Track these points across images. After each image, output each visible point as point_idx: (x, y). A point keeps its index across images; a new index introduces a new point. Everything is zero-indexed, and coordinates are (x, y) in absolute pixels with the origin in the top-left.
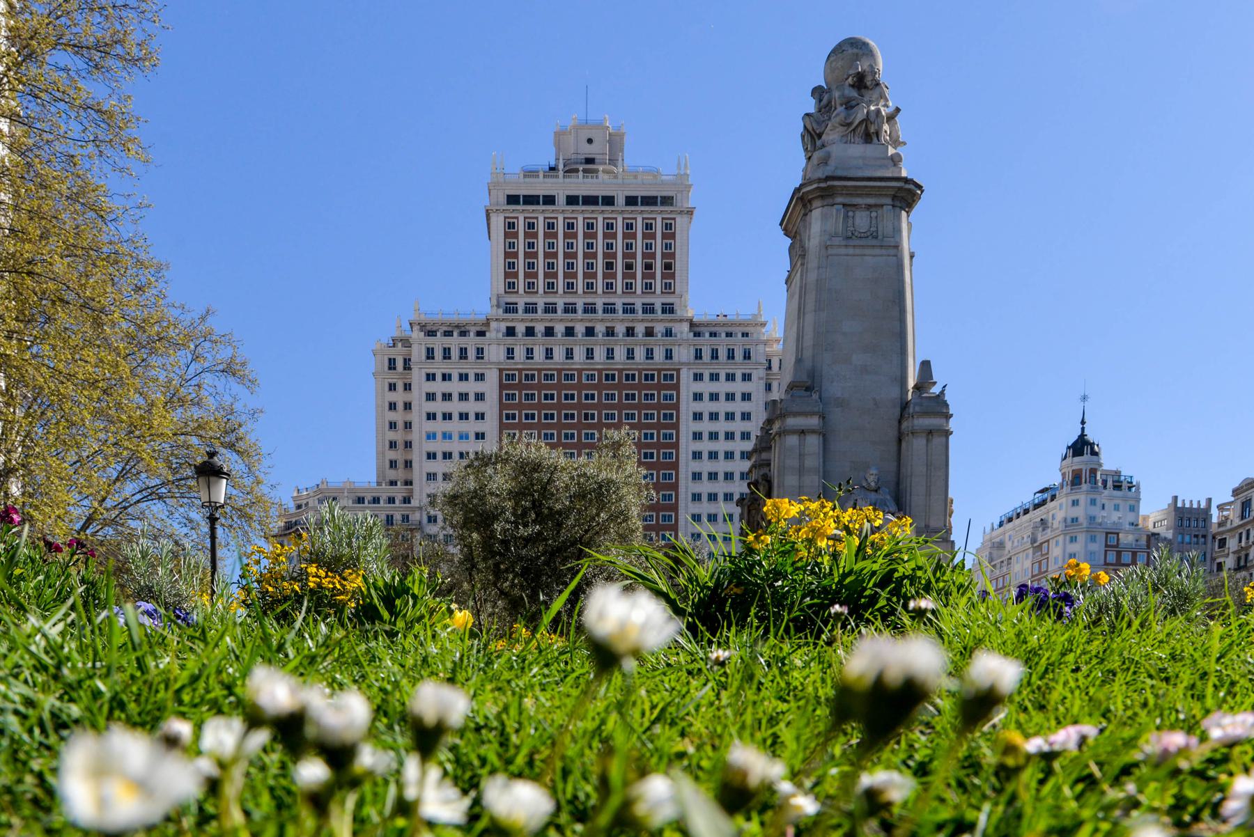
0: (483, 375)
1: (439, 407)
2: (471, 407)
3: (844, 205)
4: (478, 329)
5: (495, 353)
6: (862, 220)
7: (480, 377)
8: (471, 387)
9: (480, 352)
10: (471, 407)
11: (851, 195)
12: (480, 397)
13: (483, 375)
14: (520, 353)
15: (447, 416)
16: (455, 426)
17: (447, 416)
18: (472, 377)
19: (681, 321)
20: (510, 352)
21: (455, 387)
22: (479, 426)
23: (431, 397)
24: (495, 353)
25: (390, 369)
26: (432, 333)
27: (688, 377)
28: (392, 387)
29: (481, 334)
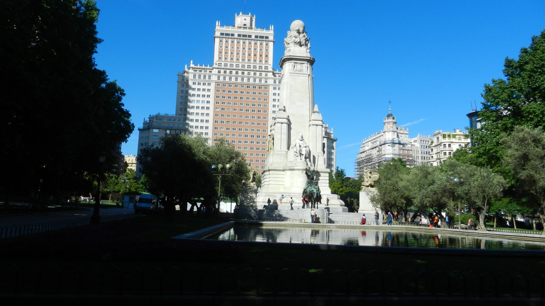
0: (210, 84)
2: (206, 93)
3: (295, 63)
4: (210, 70)
5: (214, 78)
6: (298, 66)
7: (209, 84)
8: (206, 87)
9: (210, 77)
10: (206, 93)
12: (209, 90)
13: (210, 84)
14: (222, 78)
16: (201, 99)
18: (207, 84)
19: (270, 72)
20: (219, 77)
21: (202, 87)
22: (208, 99)
24: (214, 78)
25: (182, 80)
27: (272, 88)
28: (183, 86)
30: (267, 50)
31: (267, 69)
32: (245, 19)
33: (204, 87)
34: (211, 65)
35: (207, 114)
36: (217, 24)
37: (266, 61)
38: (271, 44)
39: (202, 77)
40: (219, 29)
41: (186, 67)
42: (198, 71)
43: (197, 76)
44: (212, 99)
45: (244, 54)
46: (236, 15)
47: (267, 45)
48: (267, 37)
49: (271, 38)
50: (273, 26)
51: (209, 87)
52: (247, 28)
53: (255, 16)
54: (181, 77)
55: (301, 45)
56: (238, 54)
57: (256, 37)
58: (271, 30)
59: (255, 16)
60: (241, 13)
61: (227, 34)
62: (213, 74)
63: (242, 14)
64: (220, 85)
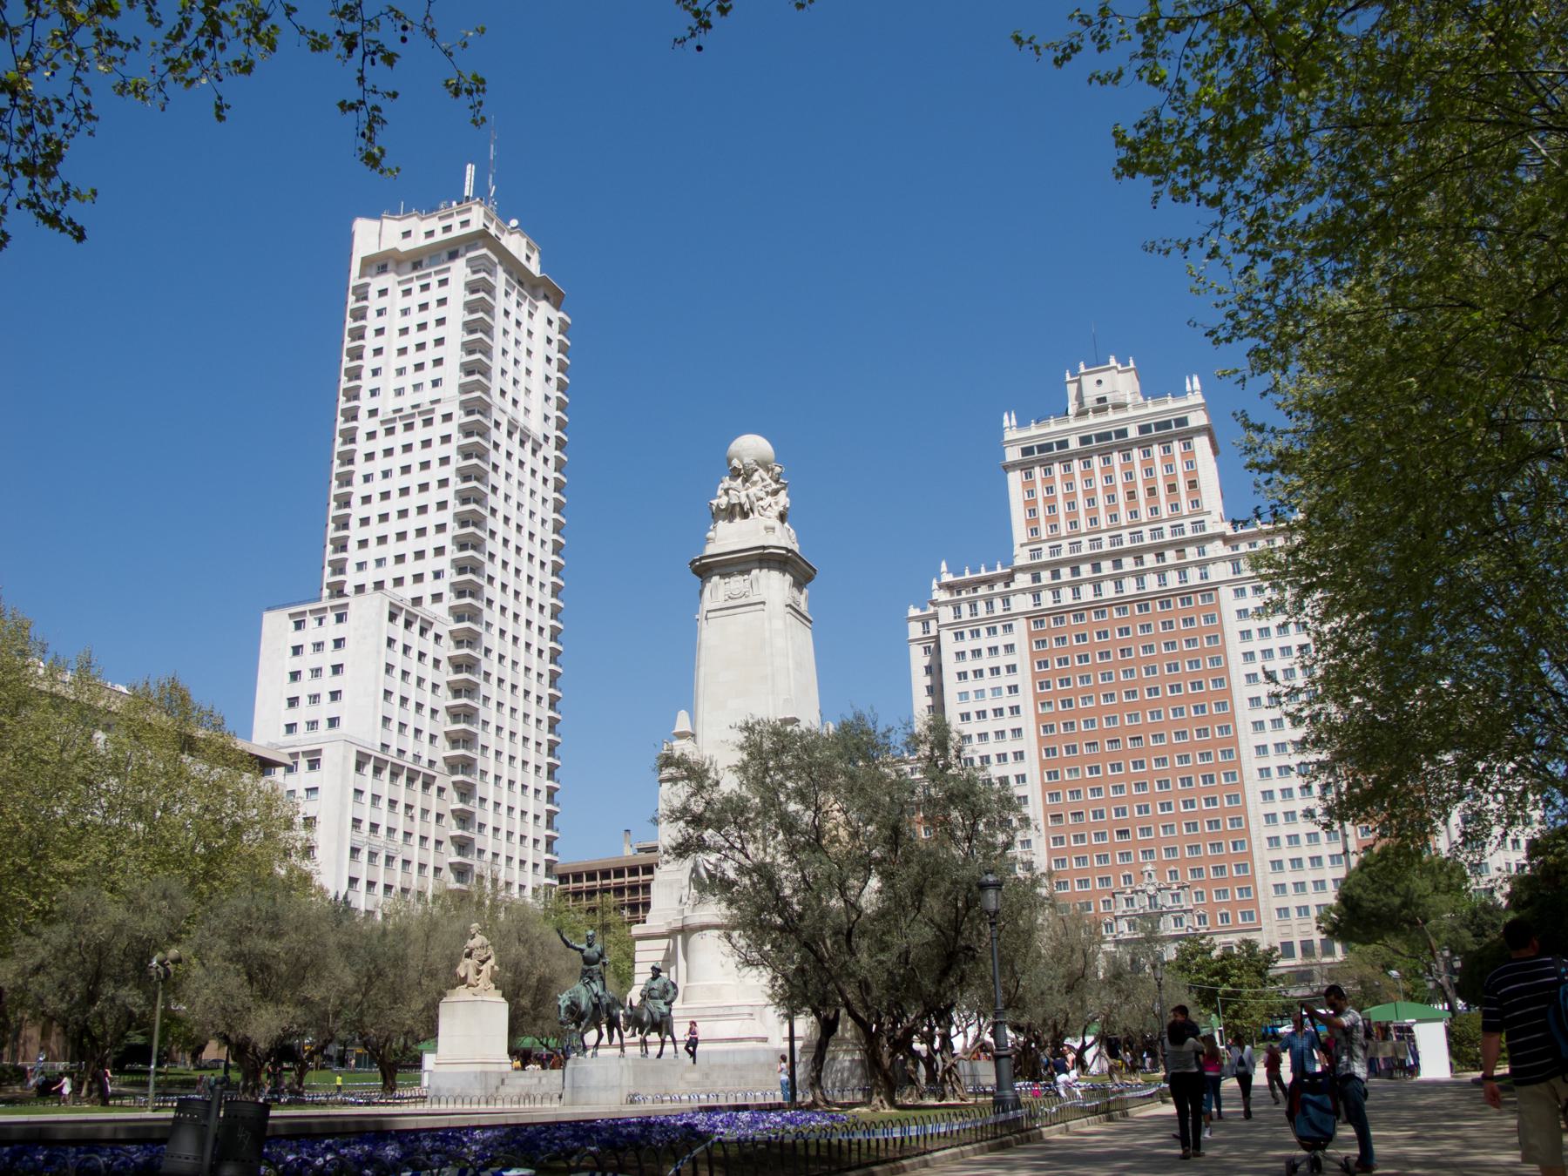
1: (969, 665)
2: (1002, 660)
5: (1022, 603)
6: (737, 583)
8: (1000, 640)
9: (1006, 601)
10: (1002, 660)
11: (725, 566)
13: (1010, 626)
14: (1047, 599)
15: (978, 673)
16: (987, 682)
17: (978, 673)
22: (1012, 680)
23: (960, 655)
24: (1022, 603)
26: (959, 593)
29: (1007, 585)
30: (1190, 464)
31: (1203, 529)
32: (1099, 382)
33: (993, 642)
34: (1008, 558)
35: (1017, 732)
36: (1006, 423)
37: (1195, 503)
38: (1201, 444)
39: (981, 606)
40: (1015, 434)
41: (935, 586)
42: (963, 592)
43: (965, 608)
44: (1024, 678)
45: (1112, 498)
46: (1068, 374)
47: (1187, 446)
48: (1182, 422)
49: (1198, 419)
50: (1195, 379)
51: (1009, 639)
52: (1105, 409)
53: (1131, 361)
54: (920, 624)
55: (745, 515)
56: (1091, 501)
57: (1144, 429)
58: (1193, 392)
59: (1131, 361)
60: (1082, 365)
61: (1042, 448)
62: (1015, 592)
63: (1086, 367)
64: (1042, 621)
